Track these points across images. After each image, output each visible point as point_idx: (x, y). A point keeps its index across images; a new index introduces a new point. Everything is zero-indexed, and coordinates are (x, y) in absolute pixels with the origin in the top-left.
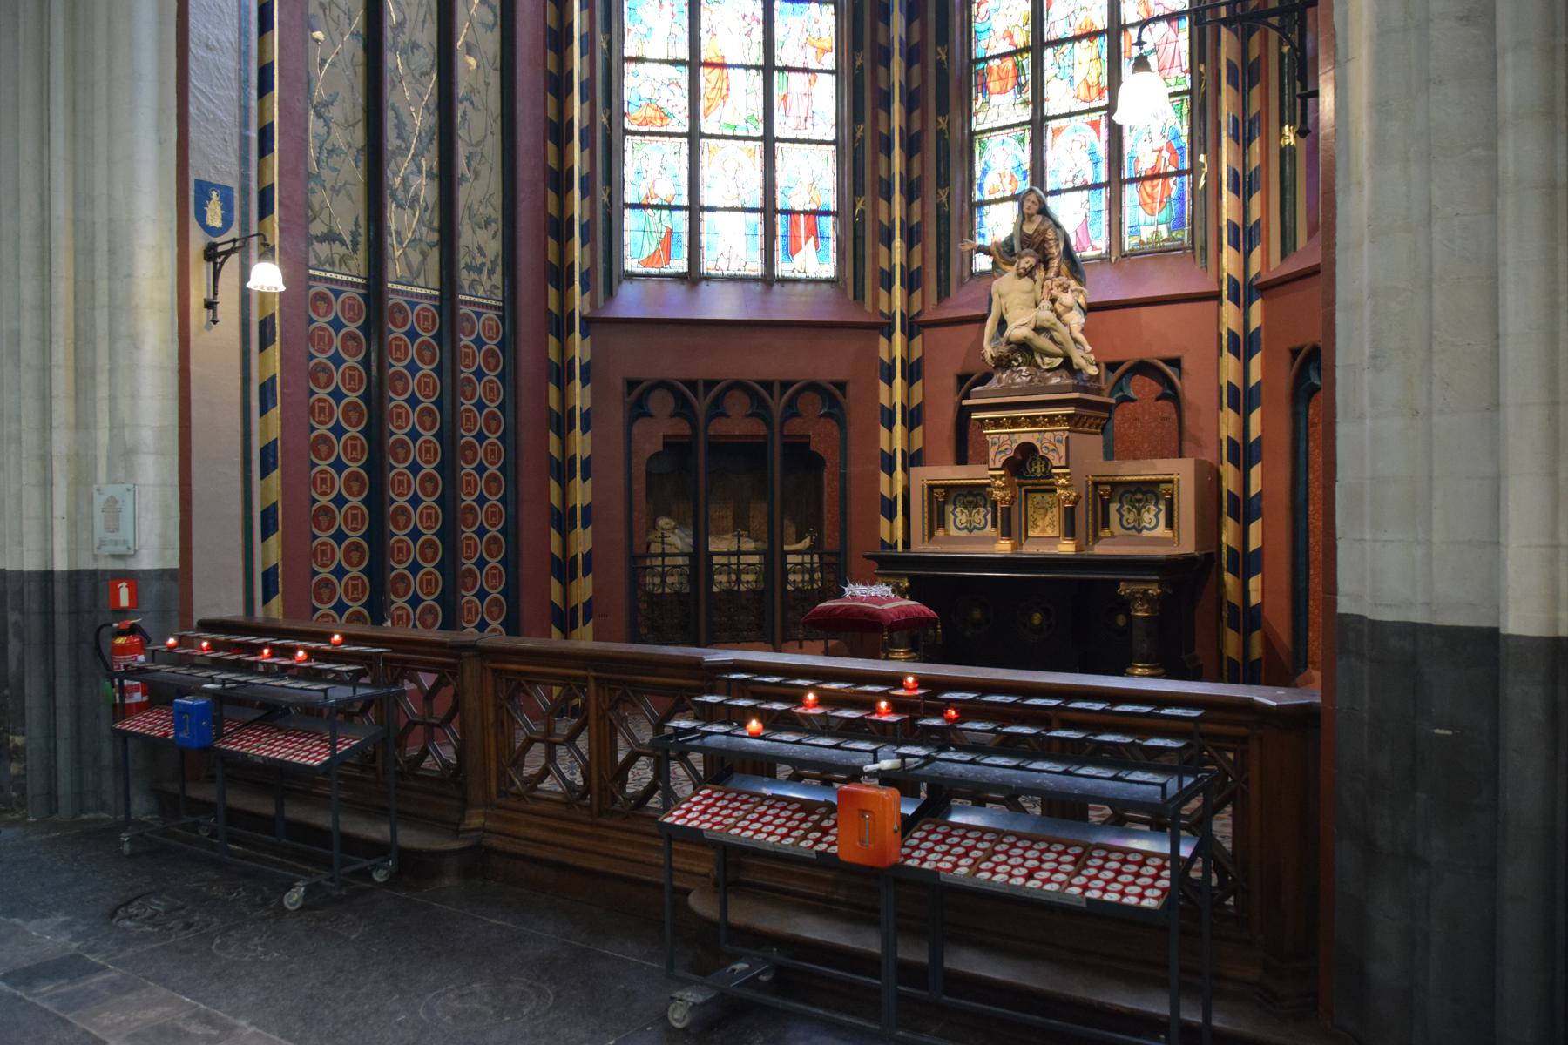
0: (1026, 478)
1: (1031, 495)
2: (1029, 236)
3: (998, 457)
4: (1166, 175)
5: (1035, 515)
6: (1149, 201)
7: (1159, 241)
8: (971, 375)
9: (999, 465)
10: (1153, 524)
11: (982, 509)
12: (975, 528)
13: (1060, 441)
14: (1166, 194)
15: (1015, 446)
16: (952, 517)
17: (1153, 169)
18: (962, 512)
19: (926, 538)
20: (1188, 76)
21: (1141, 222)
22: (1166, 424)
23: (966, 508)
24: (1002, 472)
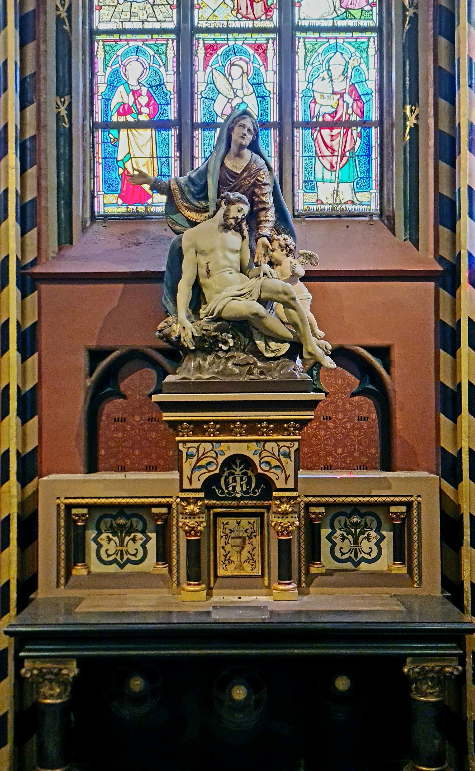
0: (219, 499)
1: (220, 520)
2: (234, 175)
3: (197, 473)
4: (348, 125)
5: (228, 548)
6: (326, 152)
8: (109, 352)
9: (198, 485)
10: (374, 554)
11: (139, 535)
12: (129, 561)
13: (287, 456)
15: (221, 459)
16: (94, 546)
17: (333, 115)
18: (109, 540)
19: (62, 581)
20: (375, 10)
22: (365, 424)
23: (114, 534)
24: (202, 495)
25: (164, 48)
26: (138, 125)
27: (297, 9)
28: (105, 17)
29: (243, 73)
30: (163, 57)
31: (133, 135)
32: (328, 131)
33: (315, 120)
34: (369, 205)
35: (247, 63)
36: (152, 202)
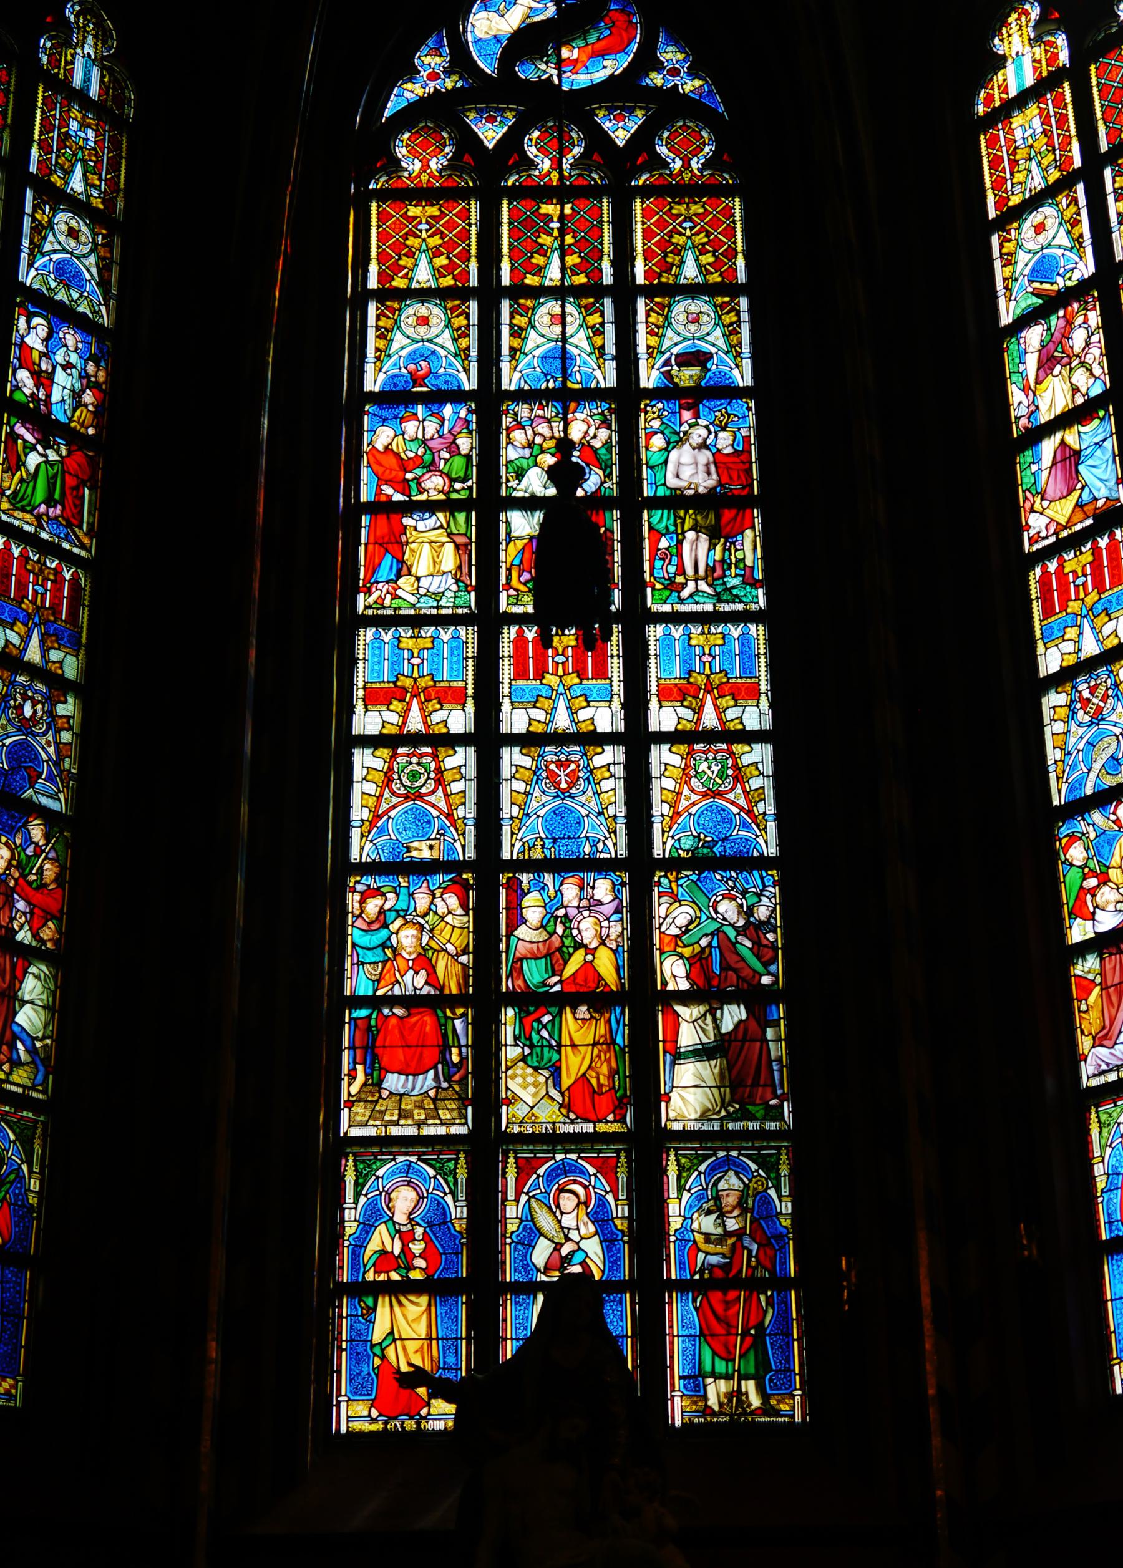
6: (719, 1329)
7: (745, 1413)
14: (753, 1321)
21: (708, 1367)
25: (451, 1165)
26: (407, 1288)
27: (663, 1104)
28: (359, 1118)
29: (579, 1203)
30: (450, 1179)
31: (401, 1304)
32: (719, 1294)
33: (697, 1277)
34: (793, 1416)
35: (586, 1187)
36: (429, 1414)
